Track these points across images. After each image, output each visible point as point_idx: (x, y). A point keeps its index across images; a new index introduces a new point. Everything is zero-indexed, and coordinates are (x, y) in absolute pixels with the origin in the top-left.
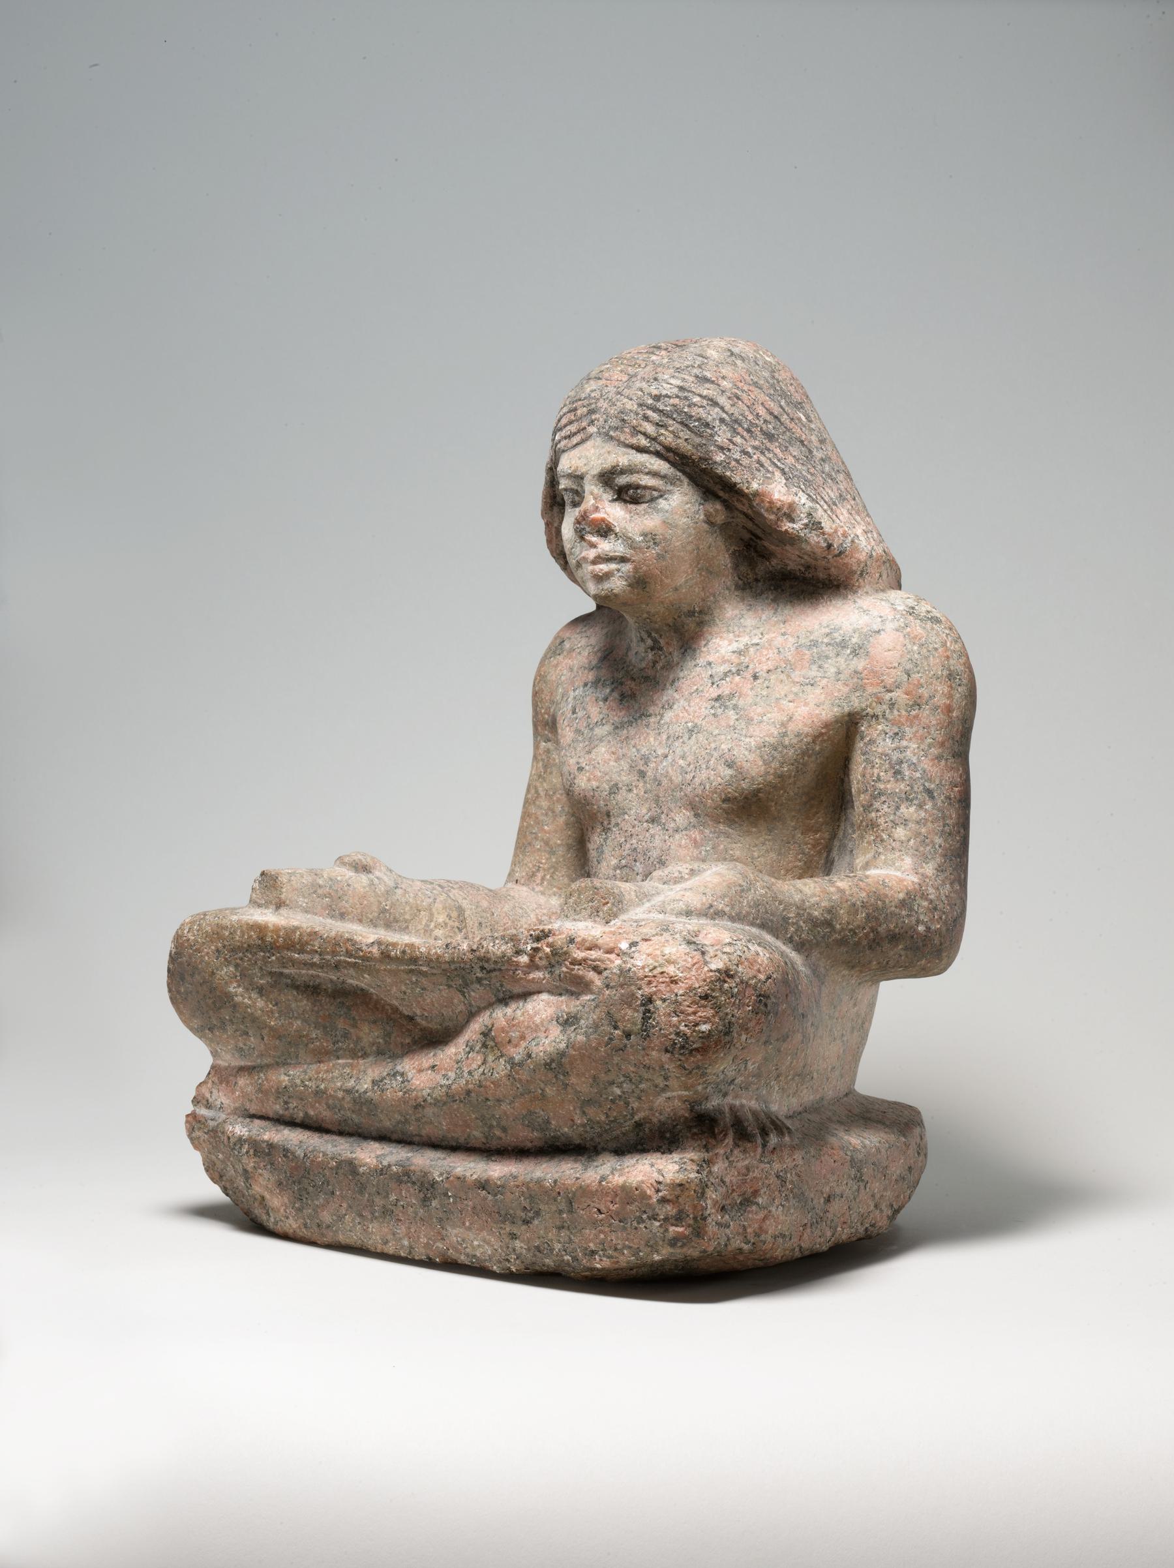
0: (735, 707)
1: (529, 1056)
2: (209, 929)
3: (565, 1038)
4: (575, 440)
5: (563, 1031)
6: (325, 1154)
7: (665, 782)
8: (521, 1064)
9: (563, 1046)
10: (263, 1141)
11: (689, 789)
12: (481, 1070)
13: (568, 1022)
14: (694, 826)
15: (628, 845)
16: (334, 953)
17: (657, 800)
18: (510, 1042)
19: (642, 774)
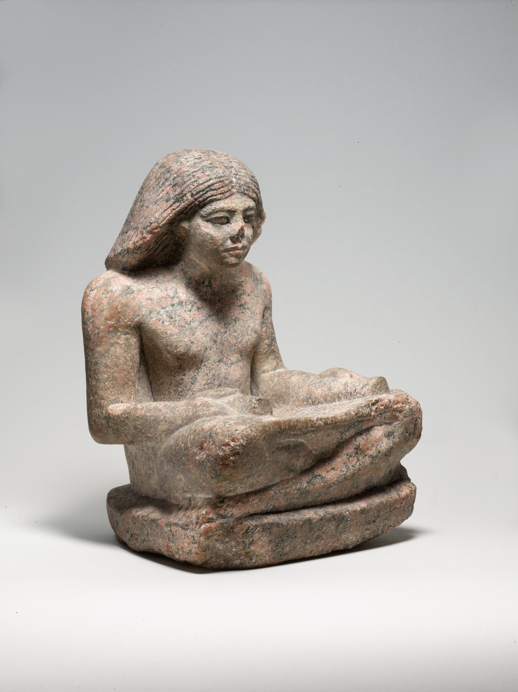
0: (248, 308)
1: (379, 452)
2: (260, 428)
3: (391, 441)
4: (227, 194)
5: (389, 439)
6: (296, 520)
7: (226, 344)
8: (376, 457)
9: (391, 445)
10: (266, 523)
11: (240, 345)
12: (358, 464)
13: (388, 435)
14: (240, 361)
15: (211, 374)
16: (307, 427)
17: (221, 353)
18: (368, 449)
19: (215, 341)
